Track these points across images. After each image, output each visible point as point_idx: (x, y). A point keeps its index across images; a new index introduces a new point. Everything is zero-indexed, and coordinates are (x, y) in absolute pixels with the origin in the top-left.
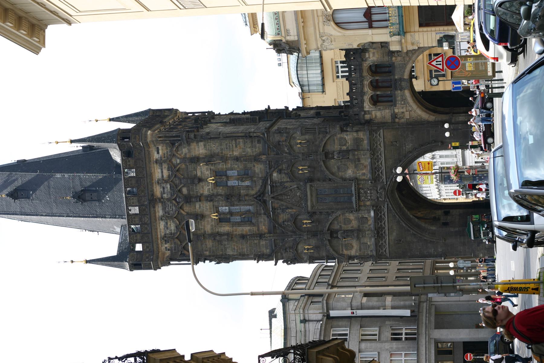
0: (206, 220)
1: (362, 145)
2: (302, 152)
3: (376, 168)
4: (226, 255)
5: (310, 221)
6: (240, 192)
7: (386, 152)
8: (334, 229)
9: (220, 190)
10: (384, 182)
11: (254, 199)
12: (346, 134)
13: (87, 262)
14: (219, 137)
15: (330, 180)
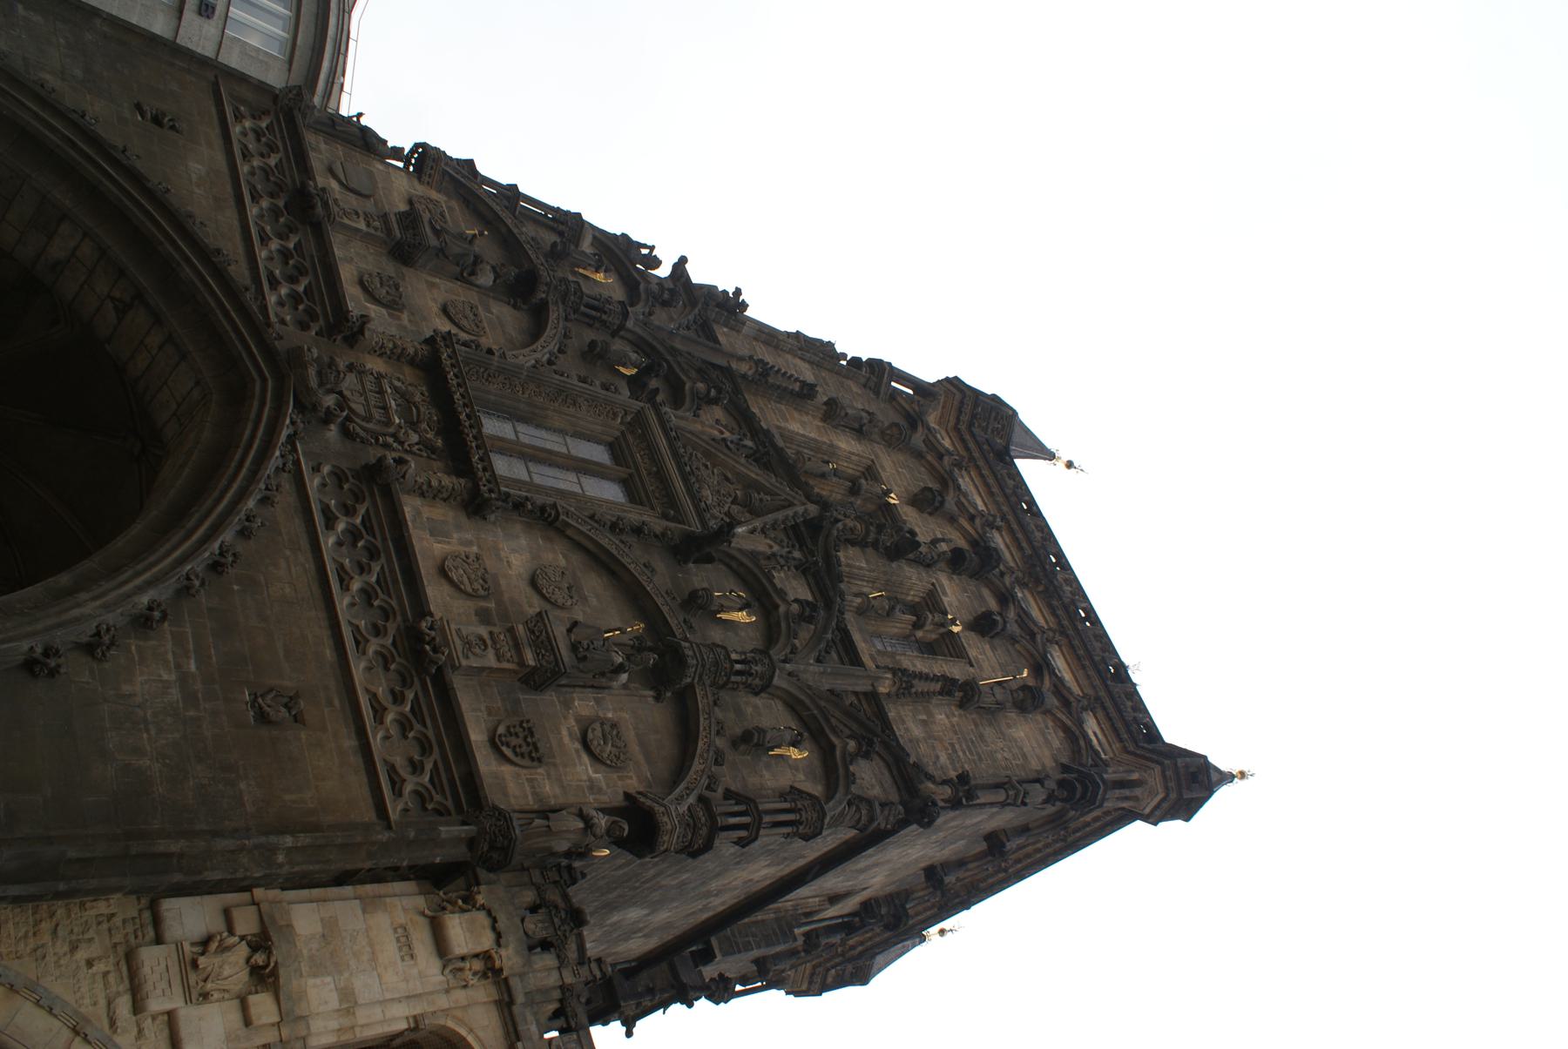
0: (903, 490)
1: (490, 714)
2: (757, 701)
3: (373, 553)
4: (810, 363)
5: (622, 369)
6: (867, 562)
7: (329, 654)
8: (515, 306)
9: (914, 581)
10: (305, 453)
11: (840, 517)
12: (600, 791)
13: (1050, 456)
14: (1024, 785)
15: (614, 527)
